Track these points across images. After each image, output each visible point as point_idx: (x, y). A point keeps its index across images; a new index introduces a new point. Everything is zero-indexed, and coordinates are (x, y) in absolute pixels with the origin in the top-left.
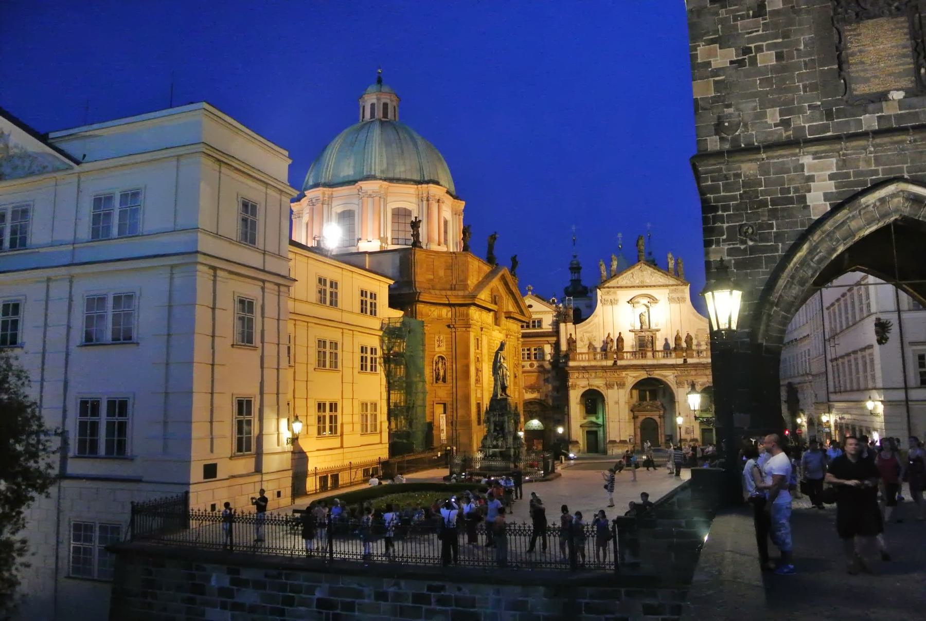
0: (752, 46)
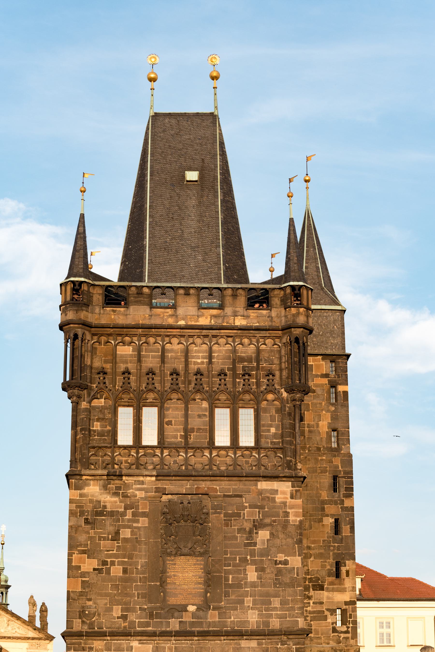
0: (109, 560)
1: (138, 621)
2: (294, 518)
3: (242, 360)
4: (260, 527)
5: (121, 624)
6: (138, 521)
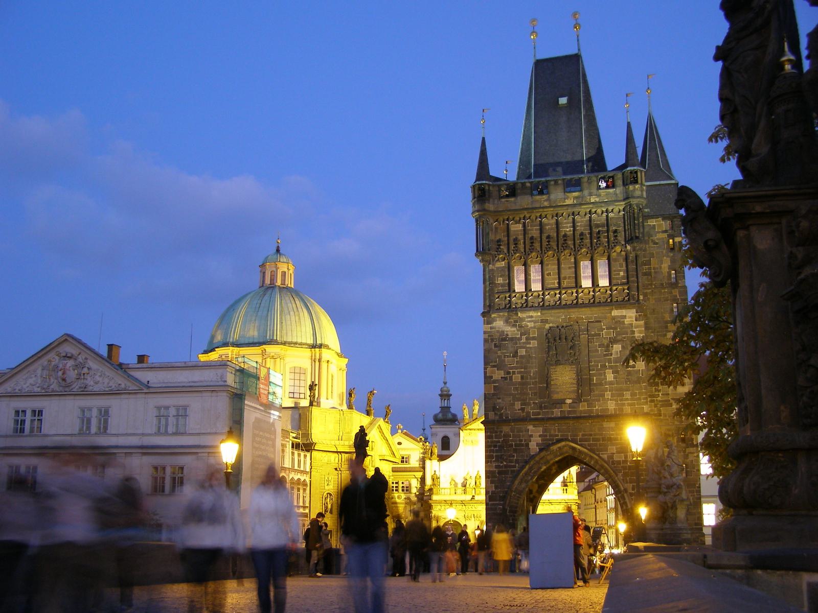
2: (638, 335)
3: (597, 226)
4: (614, 342)
6: (530, 343)
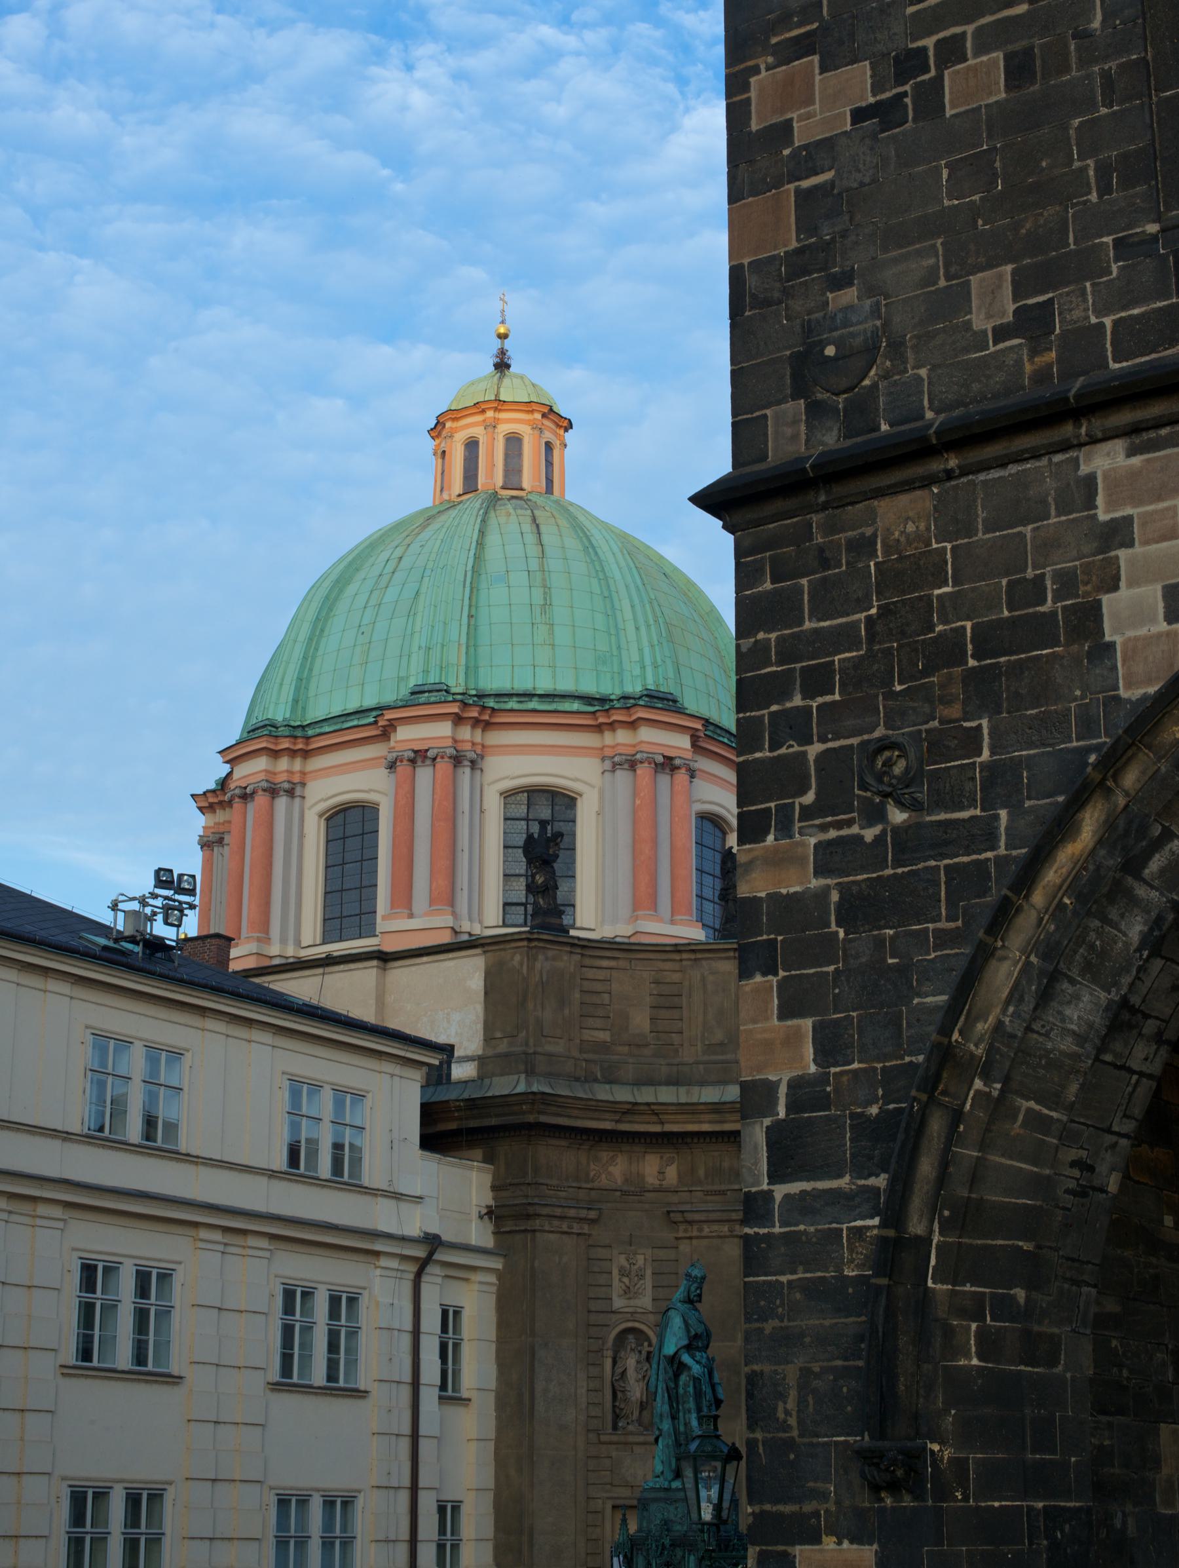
0: (929, 42)
1: (1116, 323)
5: (1019, 363)
